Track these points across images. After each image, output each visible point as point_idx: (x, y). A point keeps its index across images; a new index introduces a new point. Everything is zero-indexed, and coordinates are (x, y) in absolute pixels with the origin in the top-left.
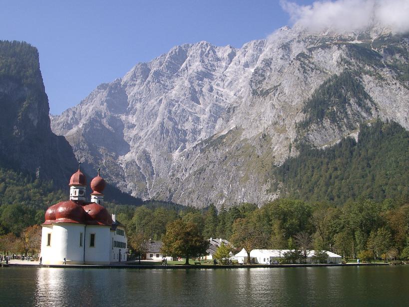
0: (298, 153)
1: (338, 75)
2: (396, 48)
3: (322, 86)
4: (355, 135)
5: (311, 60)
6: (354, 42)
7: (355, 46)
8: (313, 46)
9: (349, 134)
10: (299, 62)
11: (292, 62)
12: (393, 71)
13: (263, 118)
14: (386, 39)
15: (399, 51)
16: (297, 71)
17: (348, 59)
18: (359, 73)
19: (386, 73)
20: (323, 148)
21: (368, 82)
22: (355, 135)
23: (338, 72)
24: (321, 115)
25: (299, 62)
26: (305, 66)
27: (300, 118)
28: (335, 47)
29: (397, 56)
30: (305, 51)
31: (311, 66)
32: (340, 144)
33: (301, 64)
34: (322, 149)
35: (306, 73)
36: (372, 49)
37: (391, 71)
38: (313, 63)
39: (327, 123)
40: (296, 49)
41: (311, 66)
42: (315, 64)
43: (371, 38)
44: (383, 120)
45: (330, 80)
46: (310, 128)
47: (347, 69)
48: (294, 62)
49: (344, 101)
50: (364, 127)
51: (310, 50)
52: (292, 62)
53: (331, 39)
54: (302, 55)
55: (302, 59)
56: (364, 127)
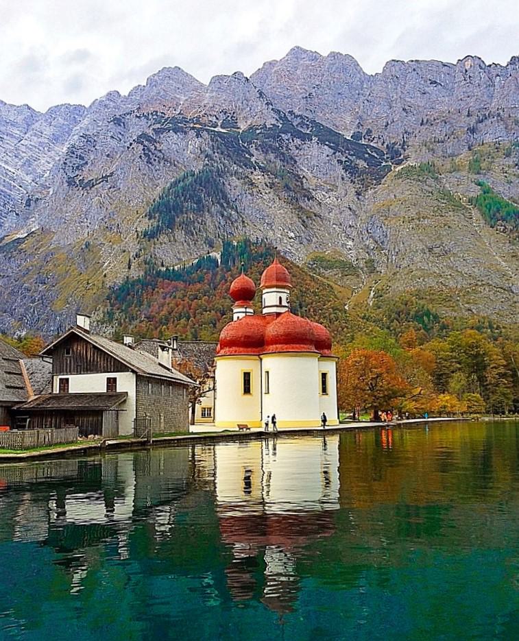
0: (142, 273)
1: (197, 172)
2: (270, 146)
3: (175, 184)
4: (217, 255)
5: (158, 145)
6: (216, 129)
7: (220, 134)
8: (158, 126)
9: (208, 253)
10: (141, 147)
11: (131, 144)
12: (266, 176)
13: (85, 220)
14: (258, 132)
15: (275, 150)
16: (138, 159)
17: (210, 152)
18: (220, 174)
19: (257, 177)
20: (176, 268)
21: (234, 186)
22: (217, 255)
23: (198, 167)
24: (171, 225)
25: (141, 147)
26: (150, 153)
27: (145, 225)
28: (192, 133)
29: (272, 156)
30: (150, 132)
31: (159, 154)
32: (199, 266)
33: (144, 150)
34: (173, 269)
35: (150, 163)
36: (241, 142)
37: (263, 175)
38: (160, 151)
39: (180, 235)
40: (136, 128)
41: (159, 154)
42: (163, 151)
43: (238, 128)
44: (253, 239)
45: (185, 178)
46: (158, 240)
47: (207, 165)
48: (134, 145)
49: (200, 209)
50: (227, 245)
51: (157, 131)
52: (131, 144)
53: (184, 120)
54: (144, 136)
55: (146, 143)
56: (227, 245)
